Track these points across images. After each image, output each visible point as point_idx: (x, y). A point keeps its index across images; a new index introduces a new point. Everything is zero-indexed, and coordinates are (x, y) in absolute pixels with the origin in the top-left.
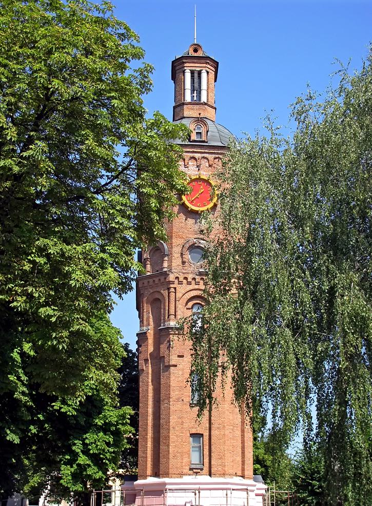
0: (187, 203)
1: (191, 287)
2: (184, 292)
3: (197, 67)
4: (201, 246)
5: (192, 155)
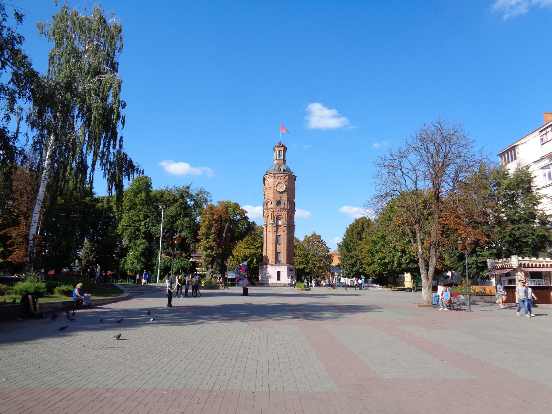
3: (280, 149)
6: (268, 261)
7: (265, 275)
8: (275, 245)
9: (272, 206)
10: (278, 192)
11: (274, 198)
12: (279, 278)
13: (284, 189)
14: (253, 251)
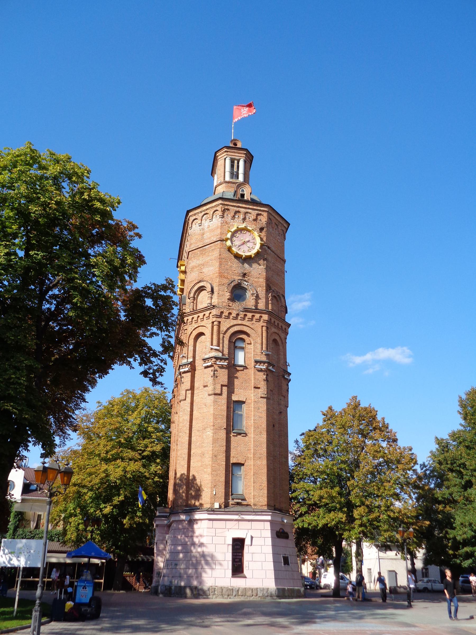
0: (233, 249)
1: (235, 322)
2: (228, 326)
4: (245, 286)
5: (238, 209)
6: (198, 496)
7: (187, 552)
8: (223, 434)
9: (215, 301)
10: (237, 256)
11: (221, 275)
12: (238, 569)
13: (257, 247)
14: (134, 467)
